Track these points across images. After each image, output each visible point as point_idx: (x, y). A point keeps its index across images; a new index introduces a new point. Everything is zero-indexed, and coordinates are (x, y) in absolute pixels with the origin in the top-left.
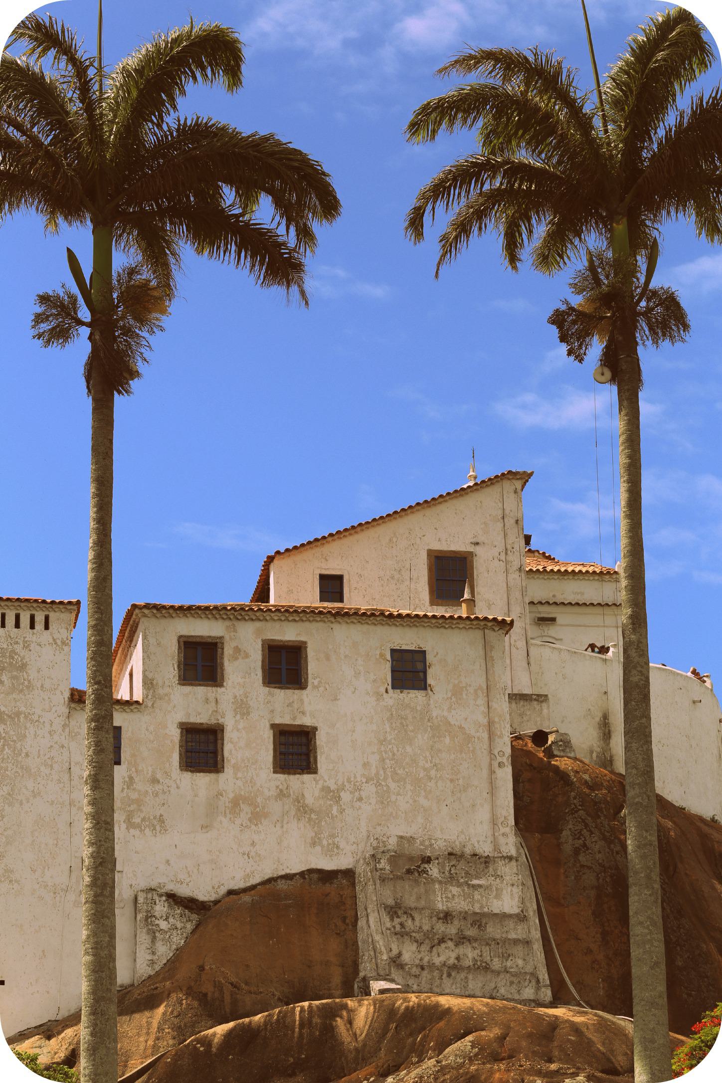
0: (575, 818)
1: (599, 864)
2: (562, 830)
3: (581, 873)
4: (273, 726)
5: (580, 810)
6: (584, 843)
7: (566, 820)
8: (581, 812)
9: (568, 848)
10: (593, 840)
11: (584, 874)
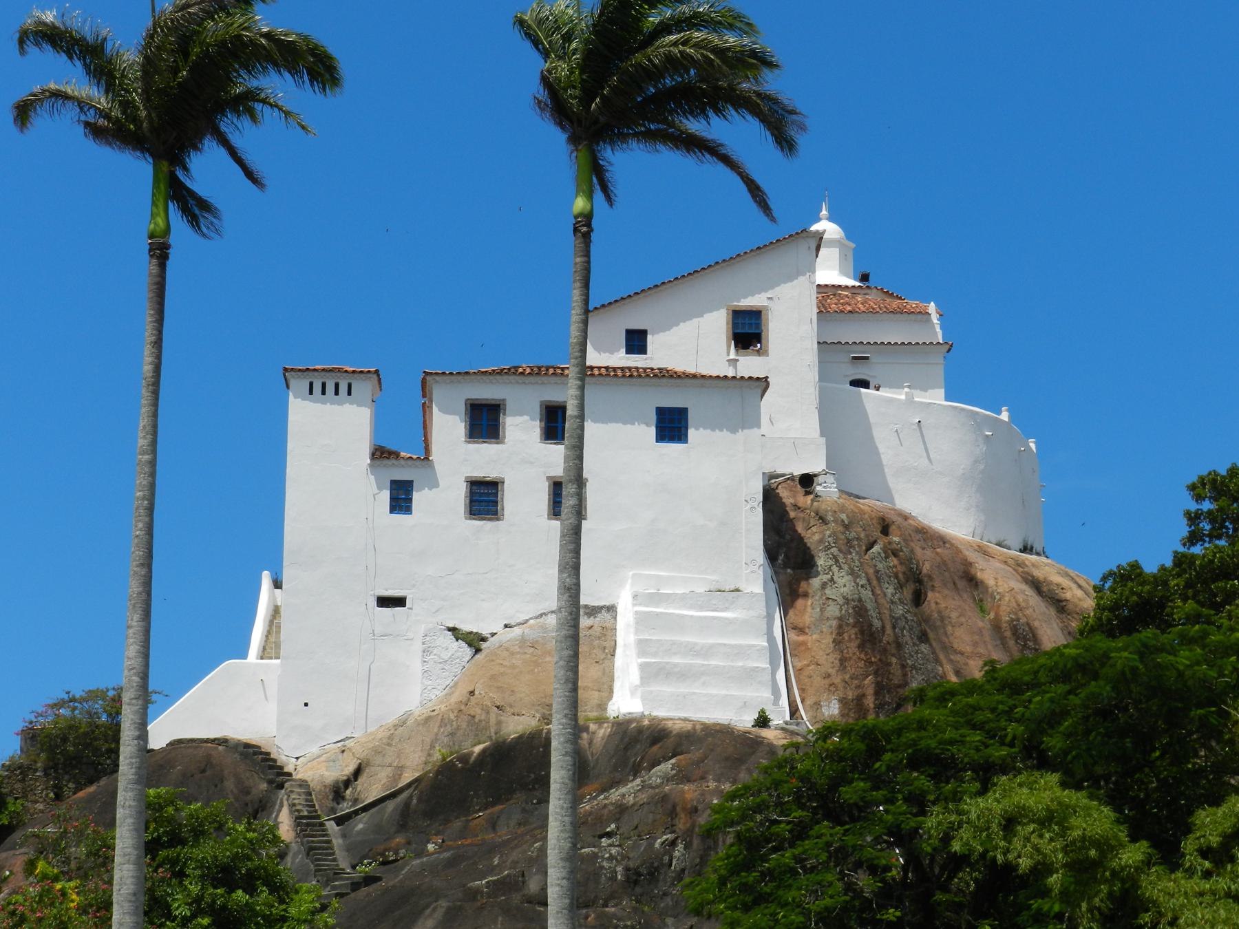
1: (844, 597)
4: (548, 478)
6: (832, 579)
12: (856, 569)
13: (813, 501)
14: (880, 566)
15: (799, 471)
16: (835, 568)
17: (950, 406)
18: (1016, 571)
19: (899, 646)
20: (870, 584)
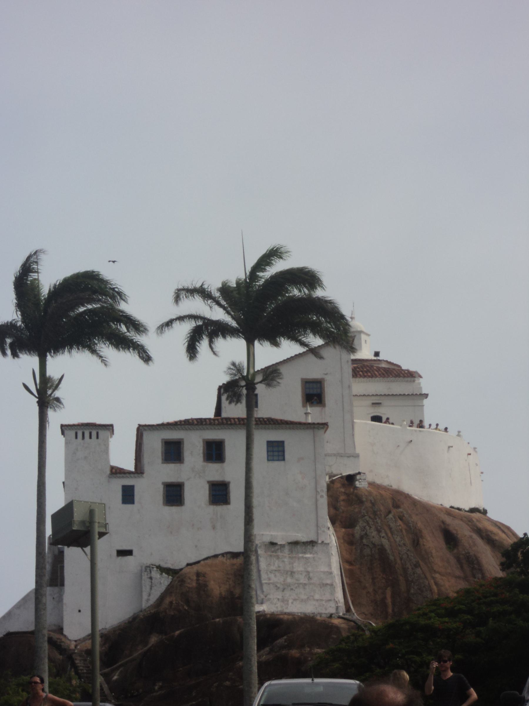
4: (208, 482)
5: (365, 516)
14: (392, 525)
16: (368, 528)
19: (405, 570)
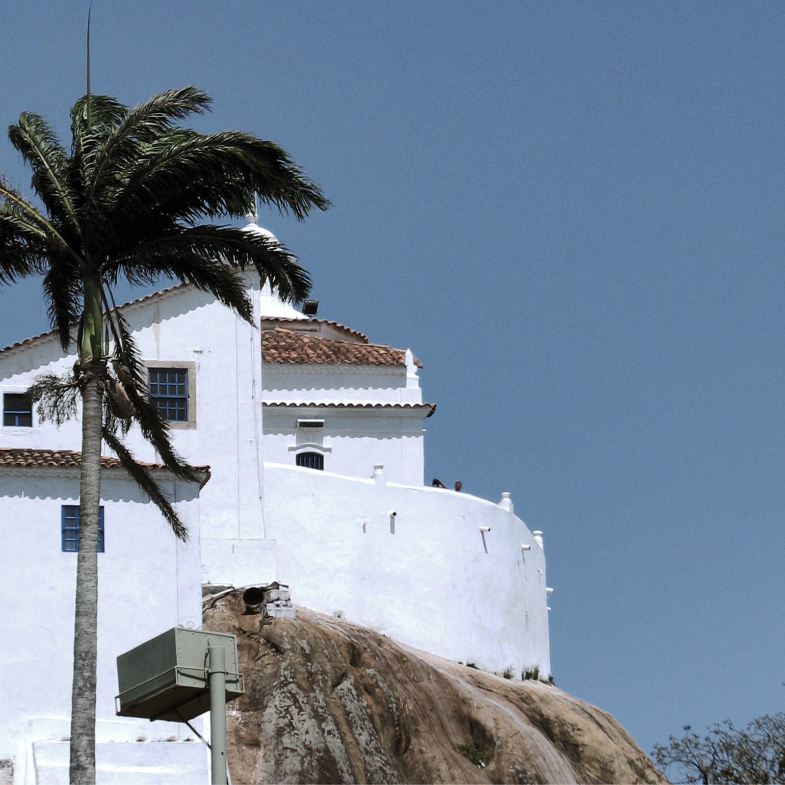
0: (284, 692)
1: (306, 747)
2: (266, 707)
3: (283, 757)
5: (290, 683)
6: (291, 723)
7: (273, 695)
8: (291, 686)
9: (269, 729)
10: (302, 719)
11: (286, 758)
12: (320, 710)
13: (262, 623)
14: (350, 706)
15: (244, 581)
16: (294, 710)
17: (435, 492)
18: (521, 709)
20: (338, 729)
